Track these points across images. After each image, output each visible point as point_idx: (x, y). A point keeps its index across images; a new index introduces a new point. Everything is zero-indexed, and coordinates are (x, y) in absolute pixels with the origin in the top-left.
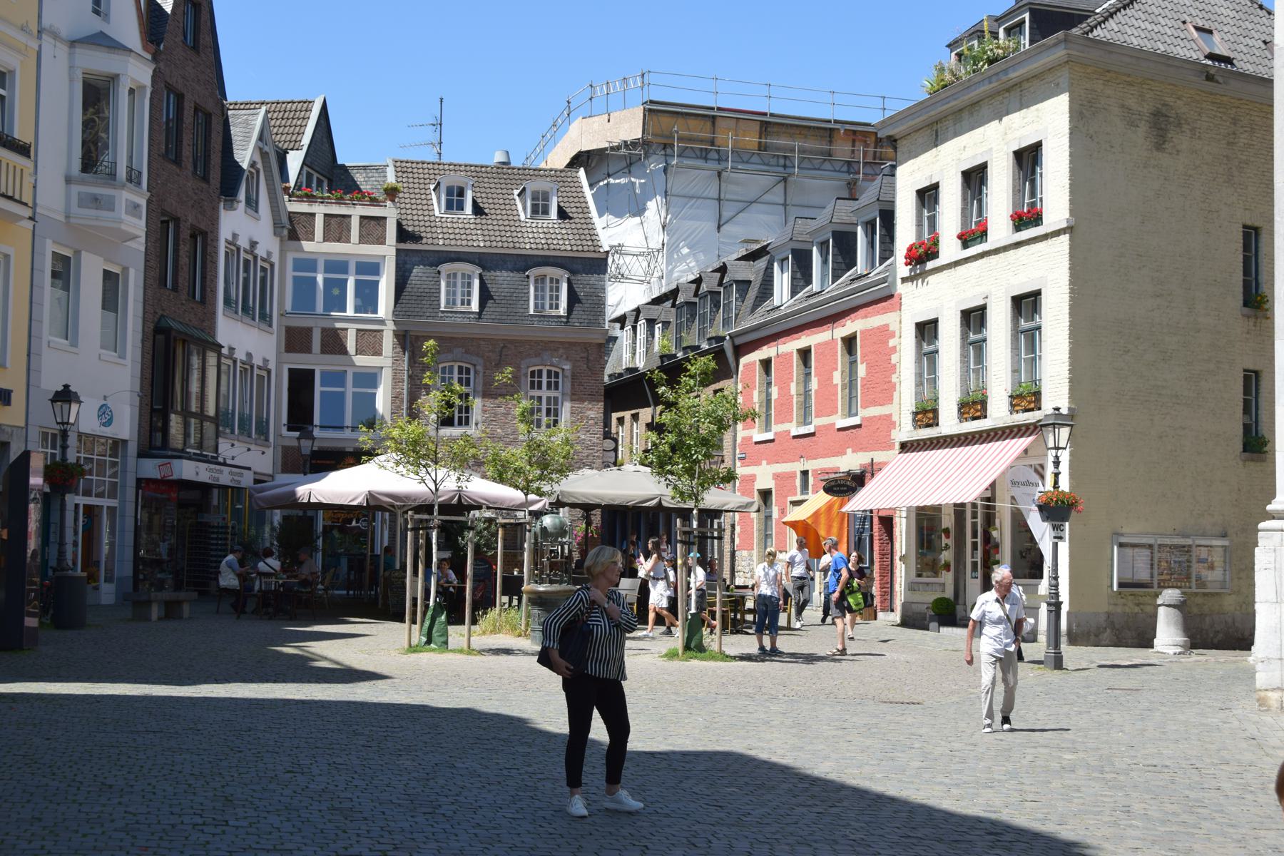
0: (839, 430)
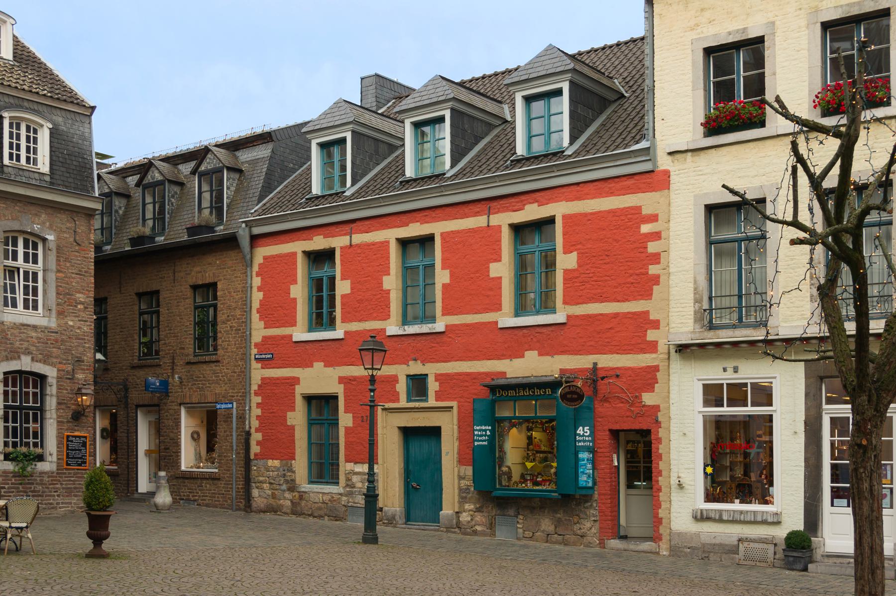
0: (501, 329)
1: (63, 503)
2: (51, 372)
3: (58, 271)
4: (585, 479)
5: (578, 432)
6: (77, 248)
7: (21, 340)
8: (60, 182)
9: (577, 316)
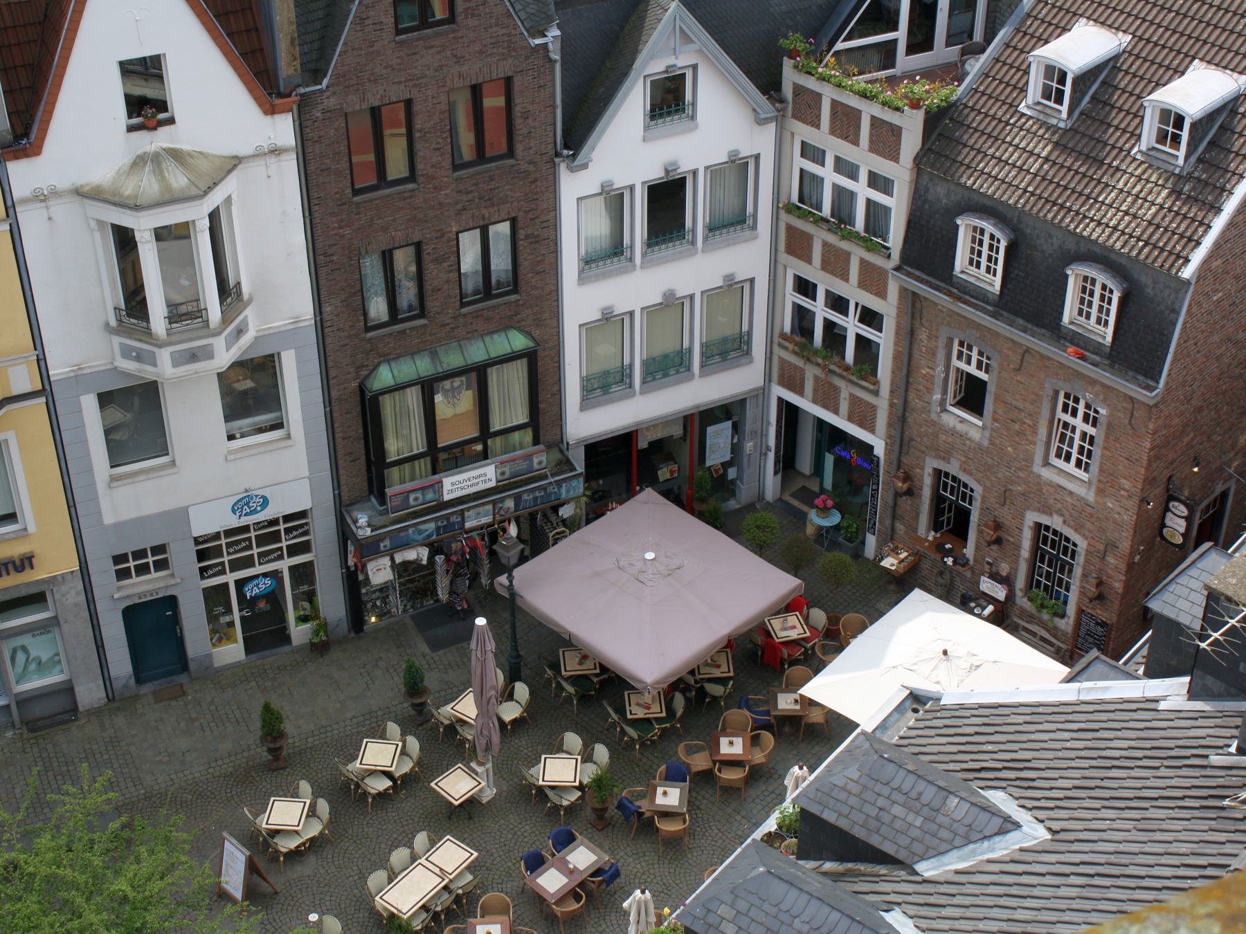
2: (1082, 544)
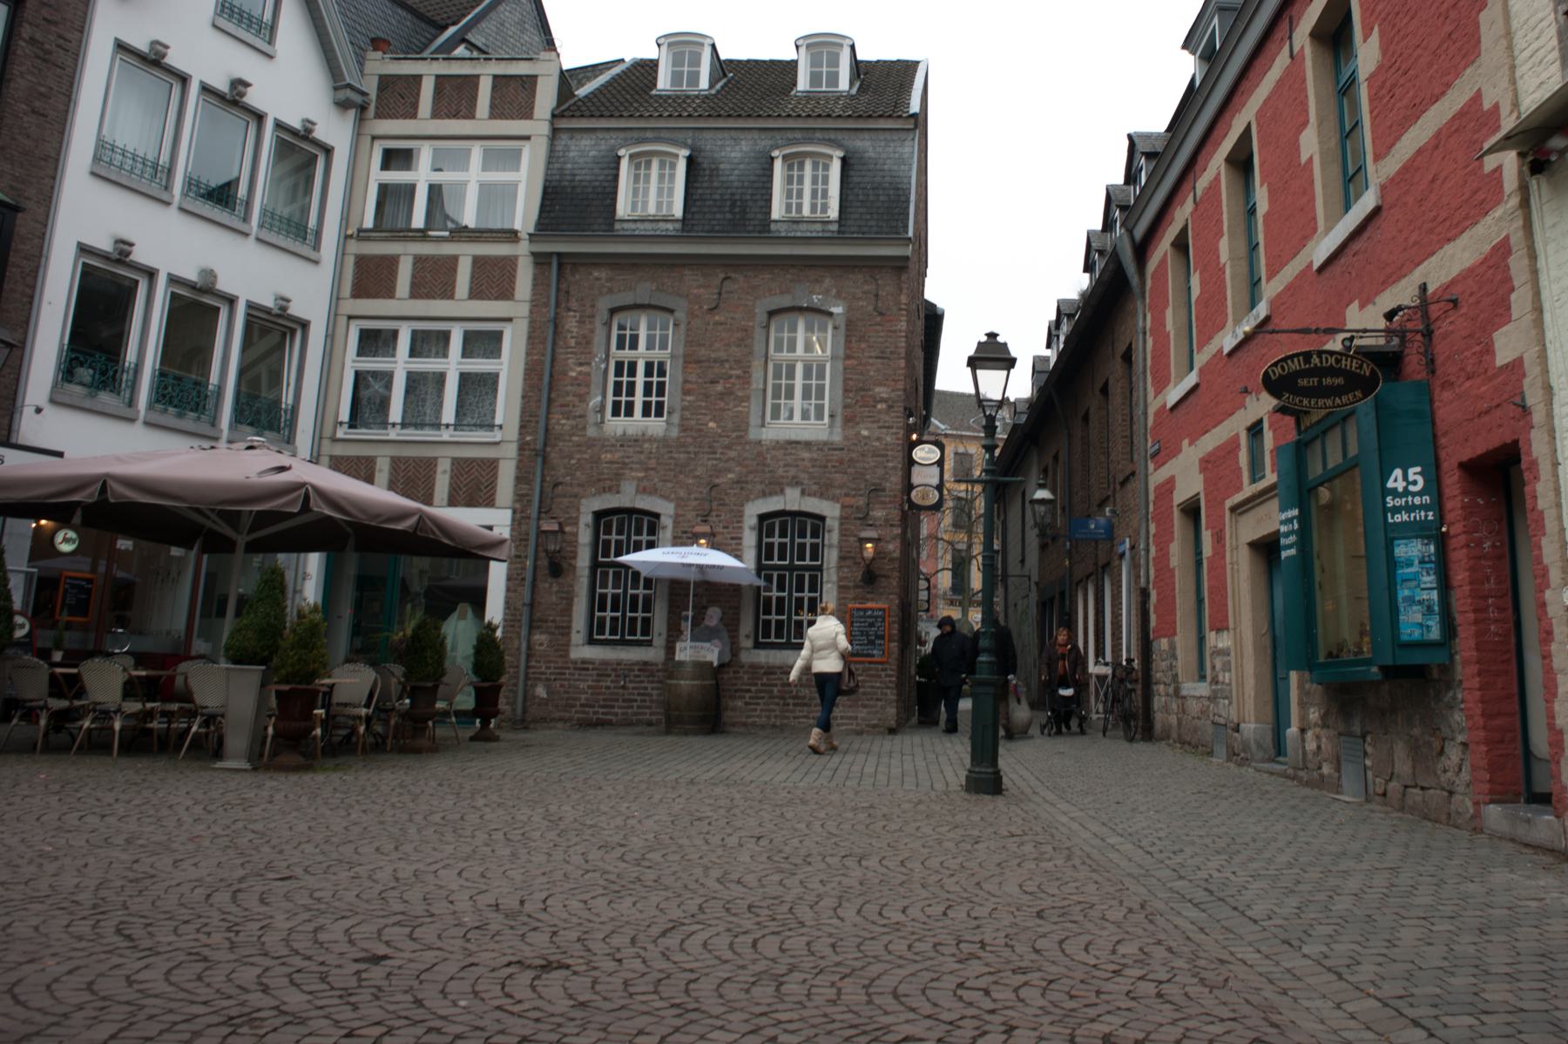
1: (842, 718)
2: (830, 510)
3: (848, 357)
4: (1418, 618)
5: (1390, 484)
6: (878, 319)
7: (785, 466)
8: (853, 229)
9: (1392, 180)
